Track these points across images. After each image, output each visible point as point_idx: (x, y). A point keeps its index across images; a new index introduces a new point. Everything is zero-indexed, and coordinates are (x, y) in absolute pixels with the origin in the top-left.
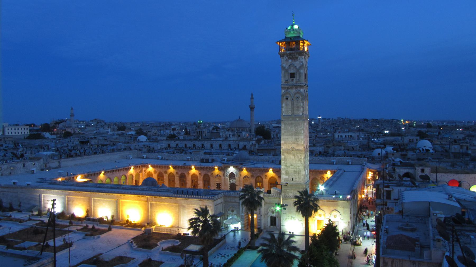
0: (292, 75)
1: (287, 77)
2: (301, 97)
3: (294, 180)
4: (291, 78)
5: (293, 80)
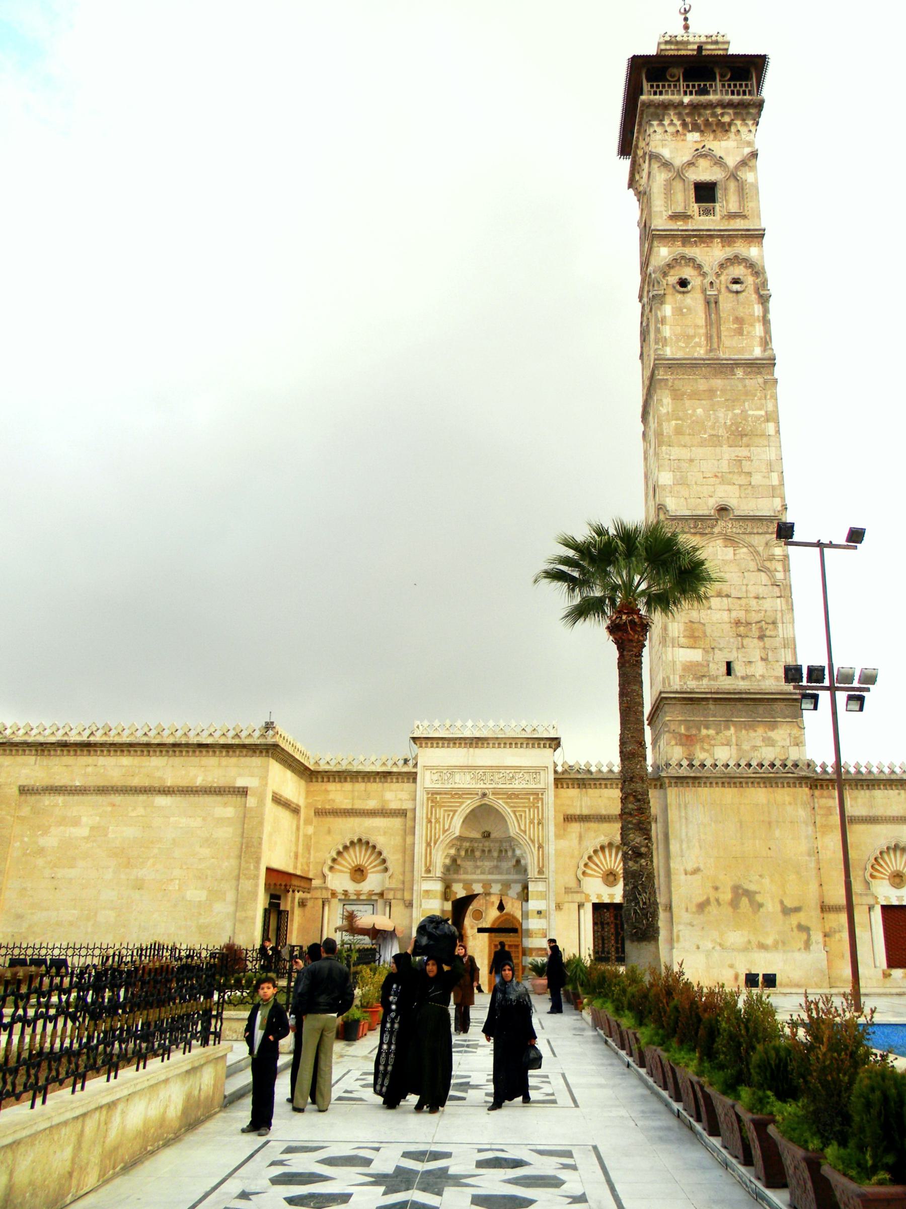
0: (705, 193)
1: (679, 197)
2: (750, 280)
3: (738, 669)
4: (698, 200)
5: (707, 212)
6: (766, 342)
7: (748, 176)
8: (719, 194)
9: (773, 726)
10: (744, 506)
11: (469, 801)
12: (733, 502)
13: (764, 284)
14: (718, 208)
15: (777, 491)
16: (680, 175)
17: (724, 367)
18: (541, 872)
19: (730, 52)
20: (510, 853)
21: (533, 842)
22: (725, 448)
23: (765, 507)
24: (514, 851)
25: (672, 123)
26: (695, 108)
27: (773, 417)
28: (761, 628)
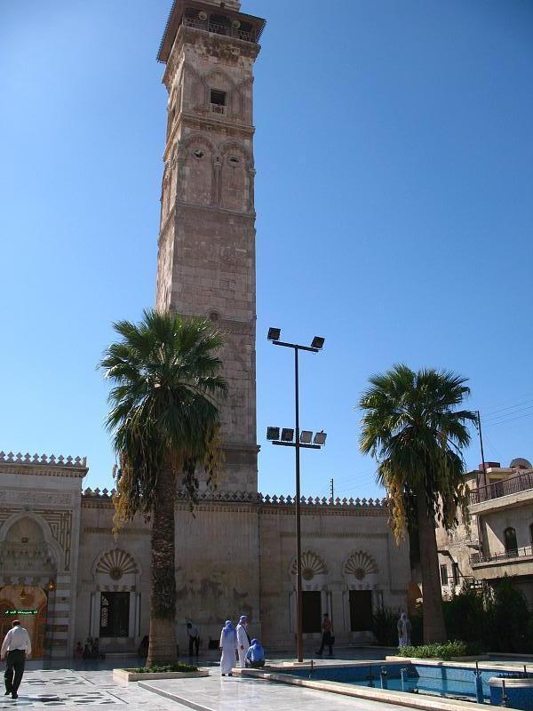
0: (218, 98)
2: (243, 160)
5: (218, 110)
6: (251, 203)
7: (247, 94)
8: (227, 100)
9: (238, 470)
10: (226, 313)
11: (15, 514)
12: (221, 310)
13: (252, 166)
14: (225, 108)
15: (251, 306)
16: (203, 80)
17: (222, 217)
18: (67, 569)
19: (240, 11)
20: (43, 555)
21: (62, 546)
22: (219, 271)
23: (241, 316)
24: (46, 553)
25: (200, 48)
26: (216, 43)
27: (252, 255)
28: (234, 400)
